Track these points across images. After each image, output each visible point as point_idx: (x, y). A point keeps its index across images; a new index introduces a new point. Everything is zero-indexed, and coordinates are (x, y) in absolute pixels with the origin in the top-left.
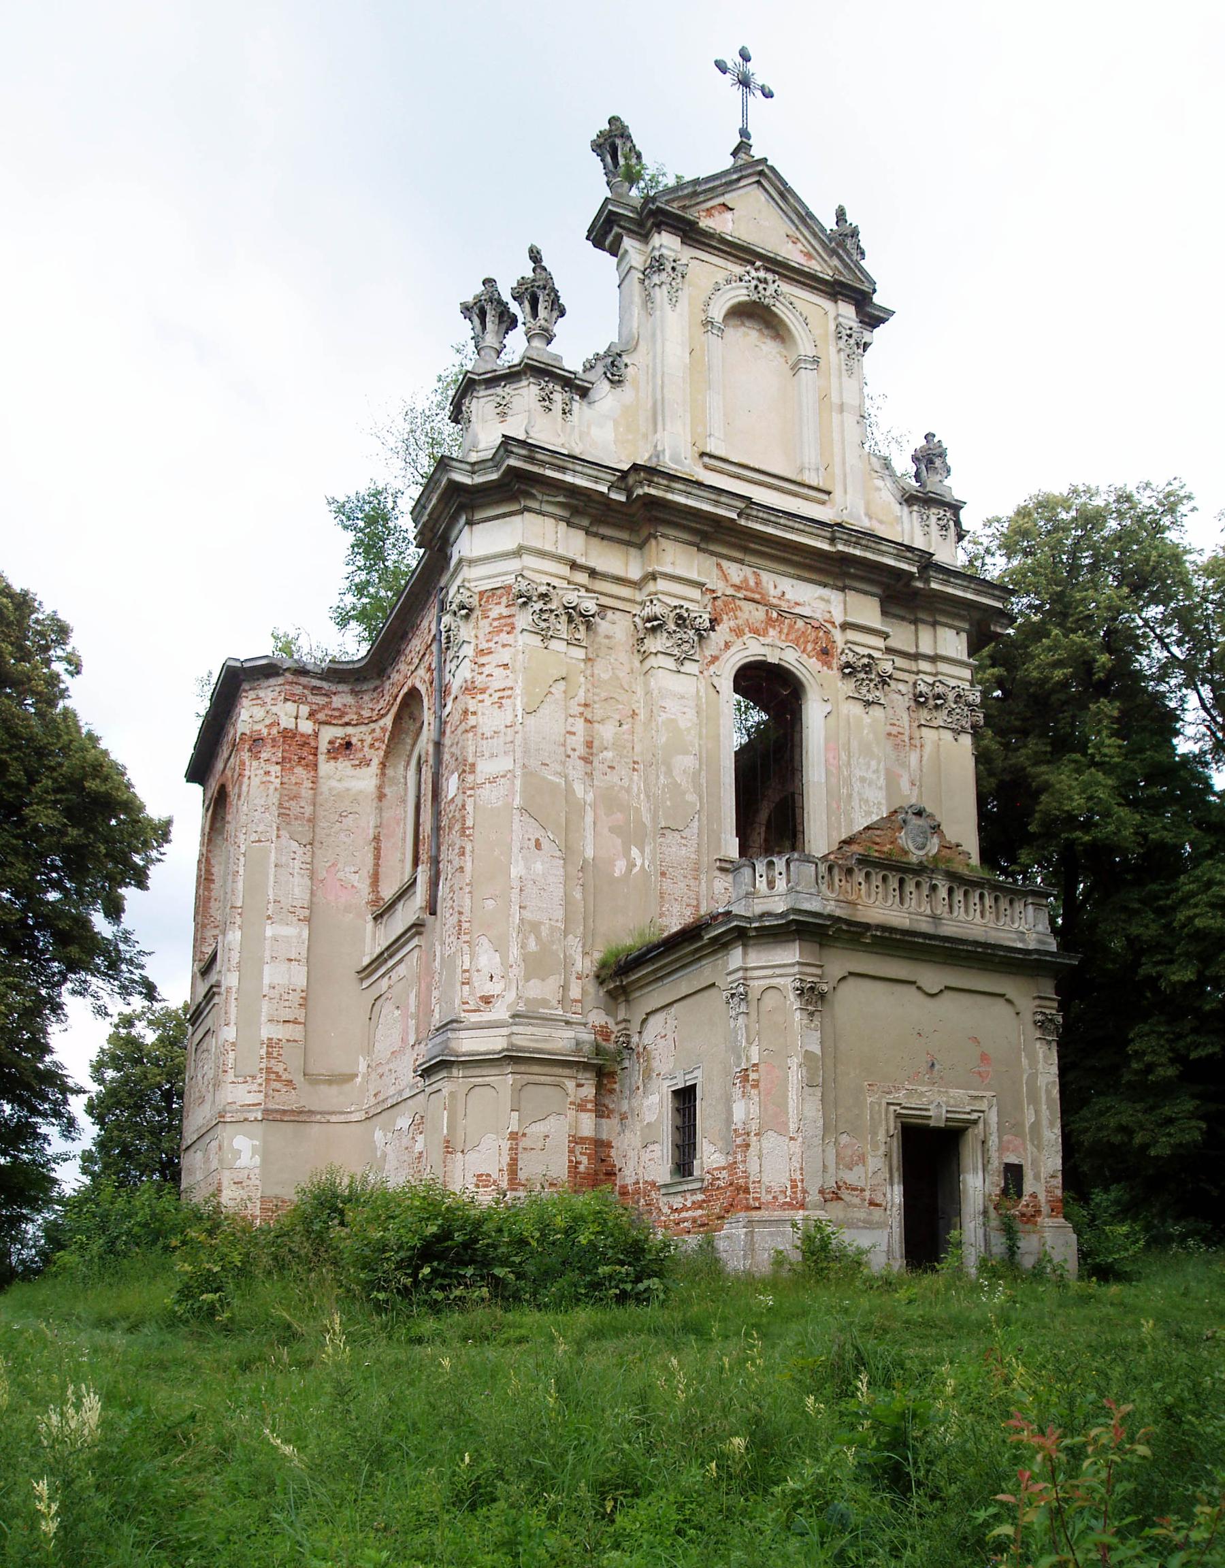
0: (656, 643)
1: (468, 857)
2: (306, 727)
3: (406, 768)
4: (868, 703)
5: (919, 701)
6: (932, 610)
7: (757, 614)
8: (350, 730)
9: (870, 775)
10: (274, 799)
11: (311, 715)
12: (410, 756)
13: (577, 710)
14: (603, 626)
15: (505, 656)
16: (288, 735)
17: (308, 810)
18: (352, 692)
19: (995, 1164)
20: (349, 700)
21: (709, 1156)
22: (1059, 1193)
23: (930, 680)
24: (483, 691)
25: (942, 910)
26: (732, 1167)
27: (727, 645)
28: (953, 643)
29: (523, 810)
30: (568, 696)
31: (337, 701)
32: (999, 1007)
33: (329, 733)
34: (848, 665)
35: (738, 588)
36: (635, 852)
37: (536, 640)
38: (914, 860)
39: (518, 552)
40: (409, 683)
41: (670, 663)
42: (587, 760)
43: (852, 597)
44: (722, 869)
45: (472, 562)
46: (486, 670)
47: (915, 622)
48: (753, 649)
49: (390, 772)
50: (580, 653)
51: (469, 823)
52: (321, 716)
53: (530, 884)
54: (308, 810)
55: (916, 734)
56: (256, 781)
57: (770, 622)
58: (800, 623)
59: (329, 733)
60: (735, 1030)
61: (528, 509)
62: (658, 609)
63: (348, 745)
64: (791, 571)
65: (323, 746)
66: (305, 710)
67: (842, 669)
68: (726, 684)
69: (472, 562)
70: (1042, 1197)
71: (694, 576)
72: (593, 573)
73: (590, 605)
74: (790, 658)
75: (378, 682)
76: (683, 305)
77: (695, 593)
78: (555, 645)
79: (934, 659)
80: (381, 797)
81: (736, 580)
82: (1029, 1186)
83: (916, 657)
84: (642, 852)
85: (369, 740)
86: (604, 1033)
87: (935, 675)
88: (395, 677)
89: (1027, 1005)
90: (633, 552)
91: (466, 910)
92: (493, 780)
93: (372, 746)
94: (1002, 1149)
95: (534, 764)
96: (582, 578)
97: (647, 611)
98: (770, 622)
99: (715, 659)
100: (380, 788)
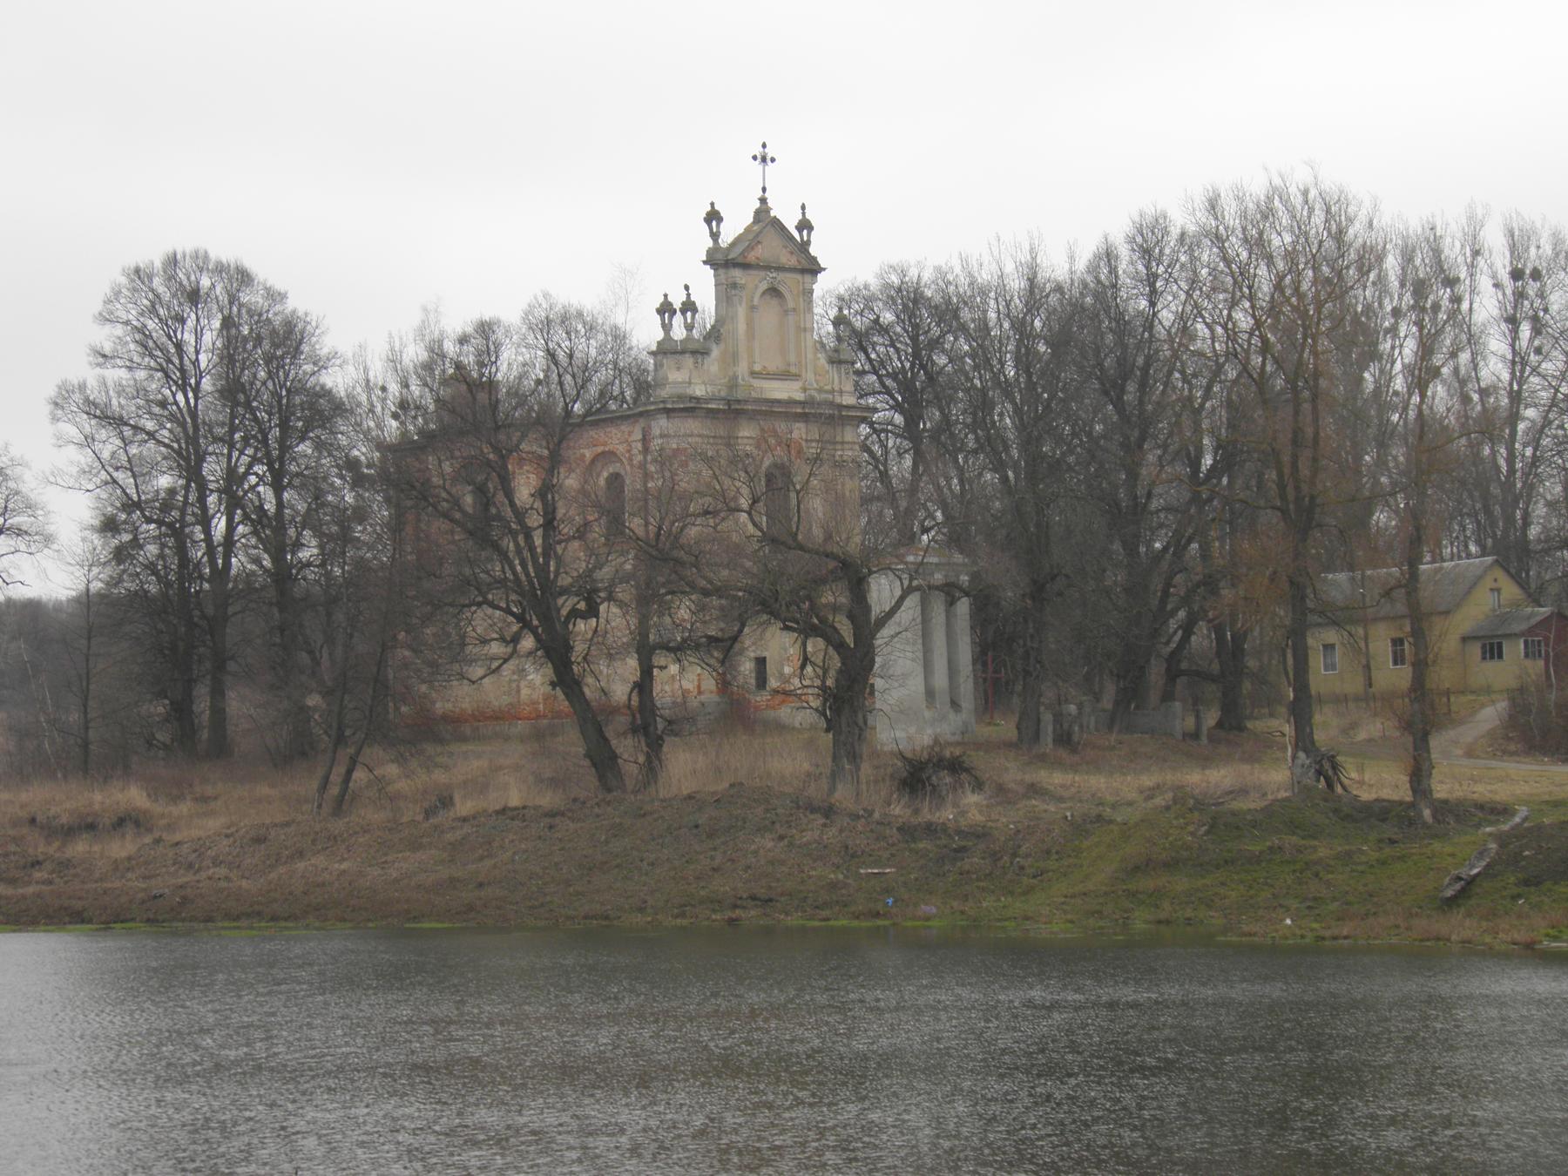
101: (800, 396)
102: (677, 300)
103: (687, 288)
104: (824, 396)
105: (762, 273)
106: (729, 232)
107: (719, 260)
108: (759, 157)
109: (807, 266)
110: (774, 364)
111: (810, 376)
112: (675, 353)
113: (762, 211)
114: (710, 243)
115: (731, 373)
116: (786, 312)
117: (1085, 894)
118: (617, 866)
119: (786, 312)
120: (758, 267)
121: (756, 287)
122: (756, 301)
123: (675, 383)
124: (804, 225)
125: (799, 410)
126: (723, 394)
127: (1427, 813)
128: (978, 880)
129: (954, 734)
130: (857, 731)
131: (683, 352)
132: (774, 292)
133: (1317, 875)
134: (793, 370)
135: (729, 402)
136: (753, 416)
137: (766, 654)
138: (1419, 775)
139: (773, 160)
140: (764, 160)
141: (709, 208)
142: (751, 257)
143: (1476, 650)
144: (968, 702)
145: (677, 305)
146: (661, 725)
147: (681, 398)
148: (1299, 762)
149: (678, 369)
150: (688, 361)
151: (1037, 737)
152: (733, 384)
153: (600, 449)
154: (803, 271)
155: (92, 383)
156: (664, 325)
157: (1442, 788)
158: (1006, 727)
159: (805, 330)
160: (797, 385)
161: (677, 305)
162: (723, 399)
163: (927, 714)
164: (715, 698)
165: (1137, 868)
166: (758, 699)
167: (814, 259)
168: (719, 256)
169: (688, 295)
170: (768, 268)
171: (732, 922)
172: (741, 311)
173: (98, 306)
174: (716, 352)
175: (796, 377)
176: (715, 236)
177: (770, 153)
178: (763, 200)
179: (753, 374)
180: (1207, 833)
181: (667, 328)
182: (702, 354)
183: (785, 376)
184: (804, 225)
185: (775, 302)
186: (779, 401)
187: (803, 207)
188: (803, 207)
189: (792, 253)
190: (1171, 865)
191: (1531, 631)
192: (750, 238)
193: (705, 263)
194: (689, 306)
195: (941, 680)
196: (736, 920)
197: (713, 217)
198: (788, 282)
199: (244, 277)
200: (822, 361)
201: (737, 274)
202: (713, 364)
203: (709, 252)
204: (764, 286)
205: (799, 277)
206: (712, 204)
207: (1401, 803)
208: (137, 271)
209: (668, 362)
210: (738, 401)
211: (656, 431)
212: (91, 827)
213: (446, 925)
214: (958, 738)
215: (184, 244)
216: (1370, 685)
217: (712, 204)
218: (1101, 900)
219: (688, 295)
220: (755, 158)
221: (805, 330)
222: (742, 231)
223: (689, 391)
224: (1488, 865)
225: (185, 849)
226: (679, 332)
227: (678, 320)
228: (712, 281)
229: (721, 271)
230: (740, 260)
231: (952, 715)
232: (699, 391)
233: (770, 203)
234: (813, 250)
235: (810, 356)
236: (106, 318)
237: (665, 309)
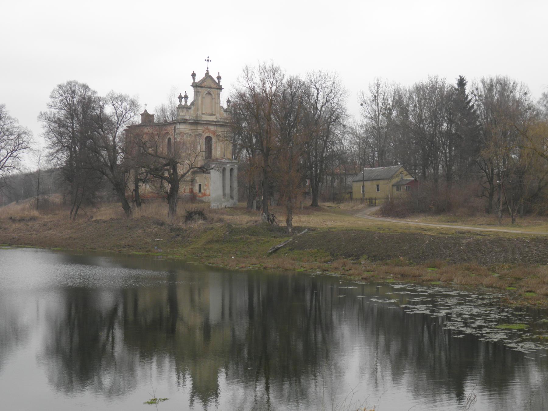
7: (207, 131)
20: (158, 128)
21: (202, 191)
39: (185, 129)
48: (207, 135)
72: (191, 129)
74: (211, 135)
76: (201, 96)
86: (192, 177)
98: (209, 132)
101: (215, 120)
102: (183, 95)
103: (186, 92)
104: (222, 120)
105: (206, 89)
106: (198, 79)
107: (195, 85)
108: (207, 60)
109: (218, 87)
110: (209, 111)
111: (218, 115)
112: (182, 108)
113: (207, 75)
115: (197, 113)
116: (212, 99)
117: (195, 248)
118: (106, 236)
119: (212, 99)
120: (204, 87)
121: (204, 92)
122: (204, 96)
123: (181, 115)
124: (219, 78)
126: (194, 119)
127: (290, 230)
128: (178, 243)
129: (231, 205)
130: (174, 203)
131: (184, 108)
132: (209, 93)
133: (248, 245)
134: (214, 113)
135: (195, 120)
136: (202, 124)
137: (201, 184)
138: (288, 221)
139: (211, 61)
140: (208, 61)
141: (193, 72)
142: (203, 85)
143: (395, 188)
144: (236, 197)
145: (183, 96)
146: (140, 201)
147: (183, 119)
148: (263, 216)
149: (183, 112)
150: (185, 110)
151: (252, 206)
152: (197, 116)
153: (166, 131)
154: (217, 89)
155: (49, 113)
156: (180, 101)
157: (294, 224)
158: (245, 204)
159: (217, 103)
160: (215, 117)
161: (183, 96)
162: (193, 120)
163: (223, 200)
164: (189, 194)
165: (209, 242)
167: (221, 86)
168: (195, 84)
169: (186, 94)
170: (207, 88)
171: (120, 251)
172: (200, 98)
173: (50, 94)
174: (193, 108)
175: (215, 115)
176: (194, 79)
177: (210, 59)
178: (207, 71)
179: (203, 114)
180: (229, 233)
181: (180, 101)
182: (189, 108)
183: (211, 114)
184: (219, 78)
185: (210, 96)
186: (209, 121)
187: (219, 73)
188: (219, 73)
189: (214, 84)
190: (217, 241)
191: (408, 184)
192: (203, 80)
193: (191, 86)
194: (186, 97)
195: (228, 191)
196: (121, 251)
197: (194, 75)
198: (213, 91)
199: (87, 87)
200: (222, 111)
201: (199, 89)
202: (192, 111)
203: (193, 84)
204: (206, 92)
205: (216, 90)
206: (194, 71)
207: (285, 226)
208: (60, 86)
209: (180, 110)
210: (197, 120)
211: (176, 128)
212: (24, 220)
213: (61, 249)
214: (232, 206)
215: (72, 79)
216: (364, 196)
217: (194, 71)
218: (198, 250)
219: (186, 94)
220: (205, 60)
221: (217, 103)
222: (202, 78)
223: (185, 118)
224: (284, 245)
225: (29, 226)
227: (183, 100)
229: (195, 88)
230: (200, 85)
231: (231, 200)
232: (187, 118)
233: (209, 72)
234: (221, 84)
235: (218, 110)
236: (52, 97)
237: (180, 98)
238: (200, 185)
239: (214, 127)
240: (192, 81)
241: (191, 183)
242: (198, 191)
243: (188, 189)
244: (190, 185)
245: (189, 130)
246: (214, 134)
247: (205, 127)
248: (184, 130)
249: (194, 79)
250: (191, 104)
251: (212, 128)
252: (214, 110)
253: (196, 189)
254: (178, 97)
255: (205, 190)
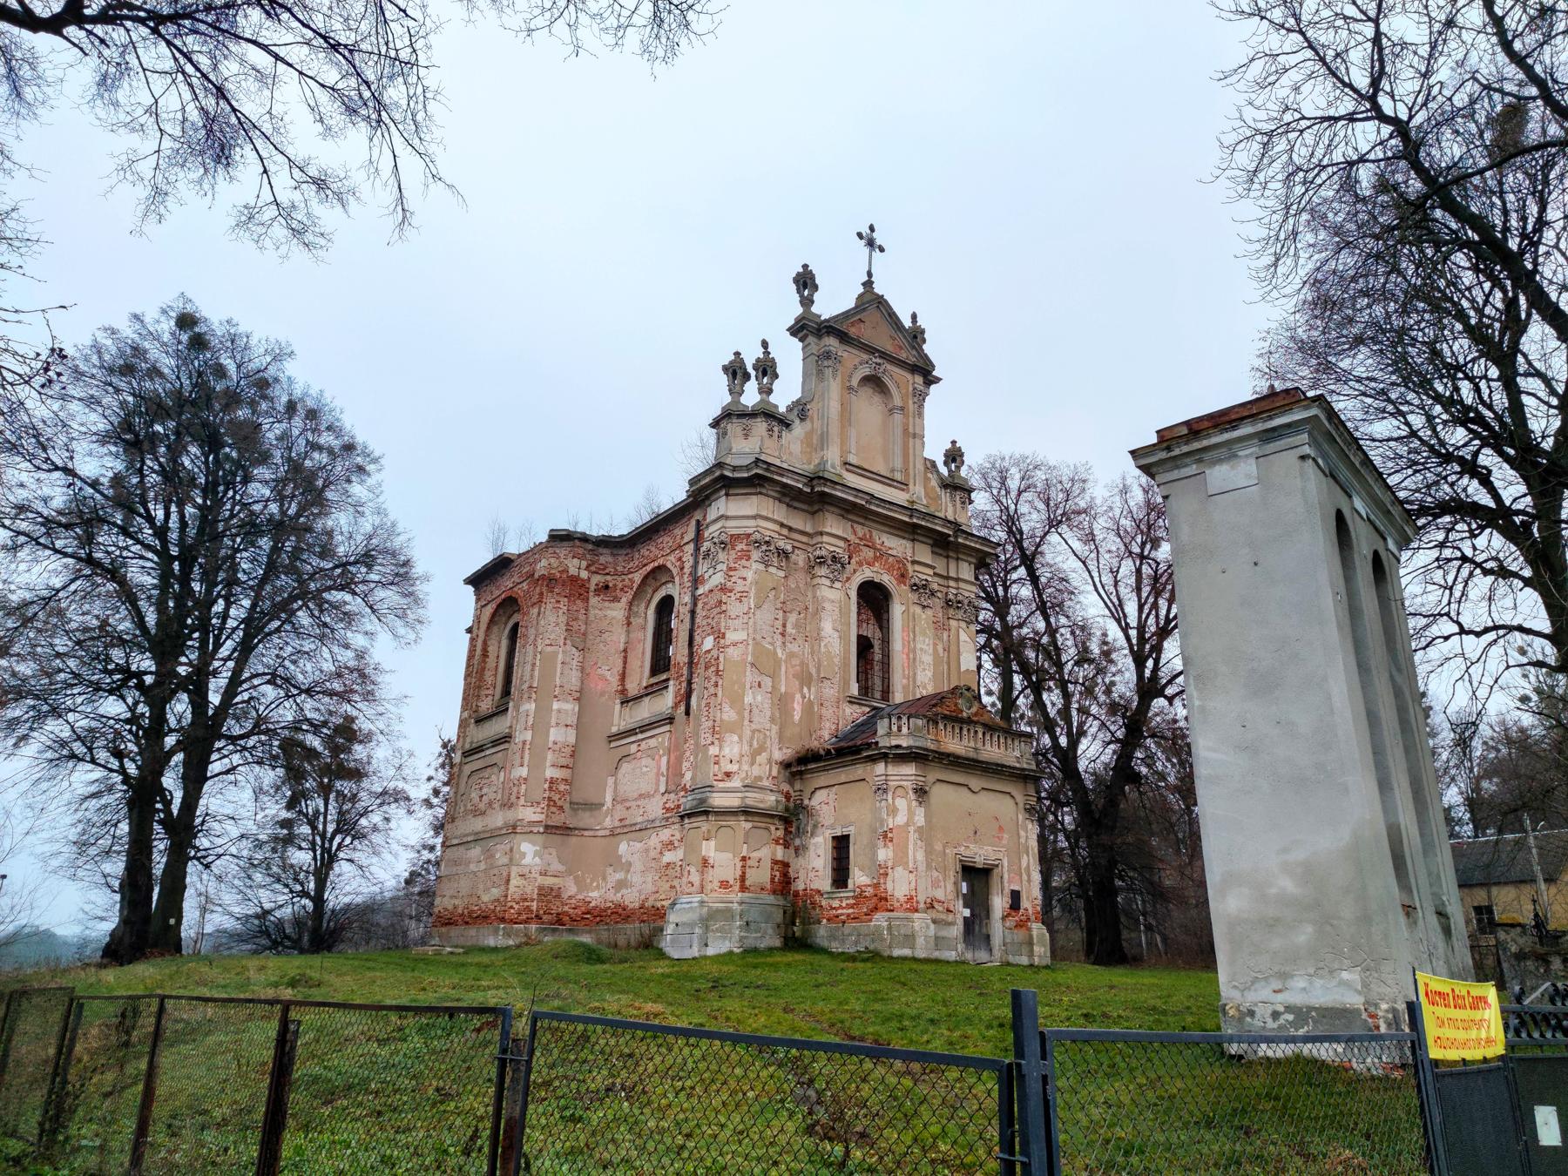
0: (823, 571)
1: (720, 688)
2: (584, 575)
3: (647, 608)
4: (924, 607)
5: (948, 603)
6: (957, 552)
8: (608, 578)
9: (925, 647)
10: (563, 619)
11: (587, 568)
12: (650, 601)
13: (779, 606)
14: (793, 557)
15: (744, 573)
16: (574, 579)
17: (583, 628)
18: (613, 555)
19: (1007, 891)
20: (610, 559)
22: (1039, 908)
23: (954, 591)
24: (731, 591)
25: (980, 745)
26: (876, 886)
27: (855, 571)
28: (966, 571)
29: (753, 665)
30: (776, 597)
31: (602, 559)
32: (1007, 800)
33: (596, 579)
34: (915, 585)
35: (861, 539)
36: (805, 690)
37: (761, 567)
38: (965, 715)
39: (754, 517)
40: (661, 561)
41: (828, 582)
42: (783, 635)
43: (918, 546)
44: (850, 702)
45: (727, 518)
46: (733, 579)
47: (947, 557)
48: (866, 574)
49: (635, 609)
50: (782, 574)
51: (721, 668)
52: (593, 568)
53: (755, 709)
54: (583, 628)
55: (946, 622)
56: (549, 606)
57: (876, 558)
58: (891, 559)
59: (596, 579)
60: (880, 808)
61: (761, 493)
62: (824, 553)
63: (607, 587)
64: (887, 529)
65: (592, 587)
66: (584, 564)
67: (911, 586)
68: (854, 595)
69: (727, 518)
70: (1030, 911)
71: (839, 533)
72: (790, 529)
73: (789, 548)
74: (886, 579)
75: (629, 551)
77: (841, 544)
78: (772, 570)
79: (957, 580)
80: (629, 624)
81: (860, 535)
82: (1025, 903)
83: (948, 578)
84: (809, 690)
85: (620, 586)
87: (958, 588)
88: (644, 552)
89: (1020, 798)
90: (809, 516)
91: (718, 719)
92: (735, 644)
93: (622, 590)
94: (1009, 882)
95: (758, 637)
96: (785, 531)
97: (818, 553)
98: (876, 558)
99: (848, 579)
100: (628, 618)
102: (751, 357)
103: (765, 344)
114: (799, 310)
116: (891, 411)
119: (891, 411)
125: (907, 519)
134: (898, 476)
137: (851, 830)
142: (853, 331)
159: (914, 436)
166: (836, 904)
169: (767, 353)
174: (799, 429)
176: (807, 302)
177: (879, 239)
181: (736, 392)
183: (888, 481)
185: (877, 399)
194: (767, 368)
197: (805, 282)
198: (897, 378)
209: (734, 428)
221: (914, 436)
226: (751, 396)
228: (800, 355)
237: (736, 372)
238: (841, 844)
239: (904, 542)
240: (799, 310)
241: (780, 833)
242: (824, 882)
243: (767, 864)
244: (777, 842)
245: (777, 528)
246: (903, 577)
247: (860, 530)
248: (752, 523)
249: (807, 302)
250: (790, 409)
251: (897, 546)
252: (898, 464)
253: (814, 868)
254: (725, 369)
255: (882, 872)
